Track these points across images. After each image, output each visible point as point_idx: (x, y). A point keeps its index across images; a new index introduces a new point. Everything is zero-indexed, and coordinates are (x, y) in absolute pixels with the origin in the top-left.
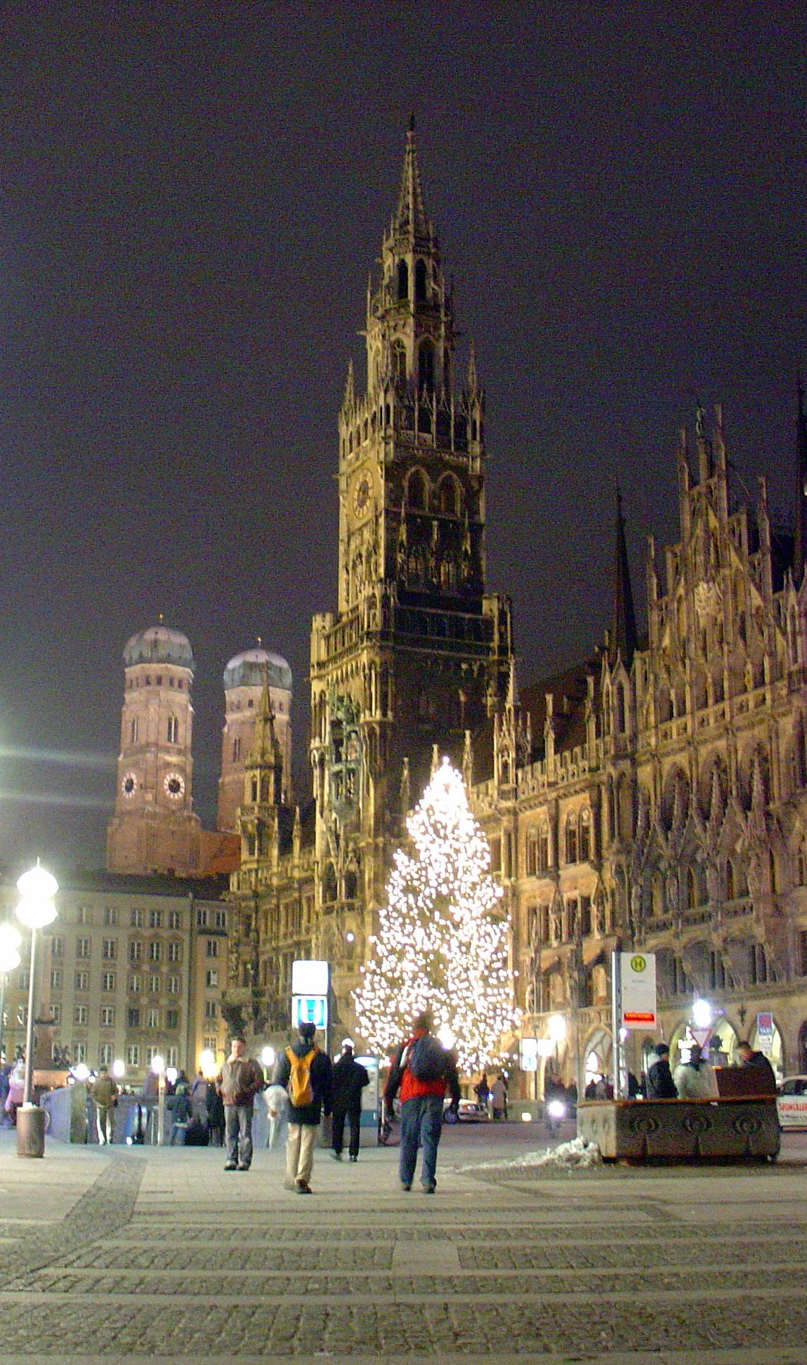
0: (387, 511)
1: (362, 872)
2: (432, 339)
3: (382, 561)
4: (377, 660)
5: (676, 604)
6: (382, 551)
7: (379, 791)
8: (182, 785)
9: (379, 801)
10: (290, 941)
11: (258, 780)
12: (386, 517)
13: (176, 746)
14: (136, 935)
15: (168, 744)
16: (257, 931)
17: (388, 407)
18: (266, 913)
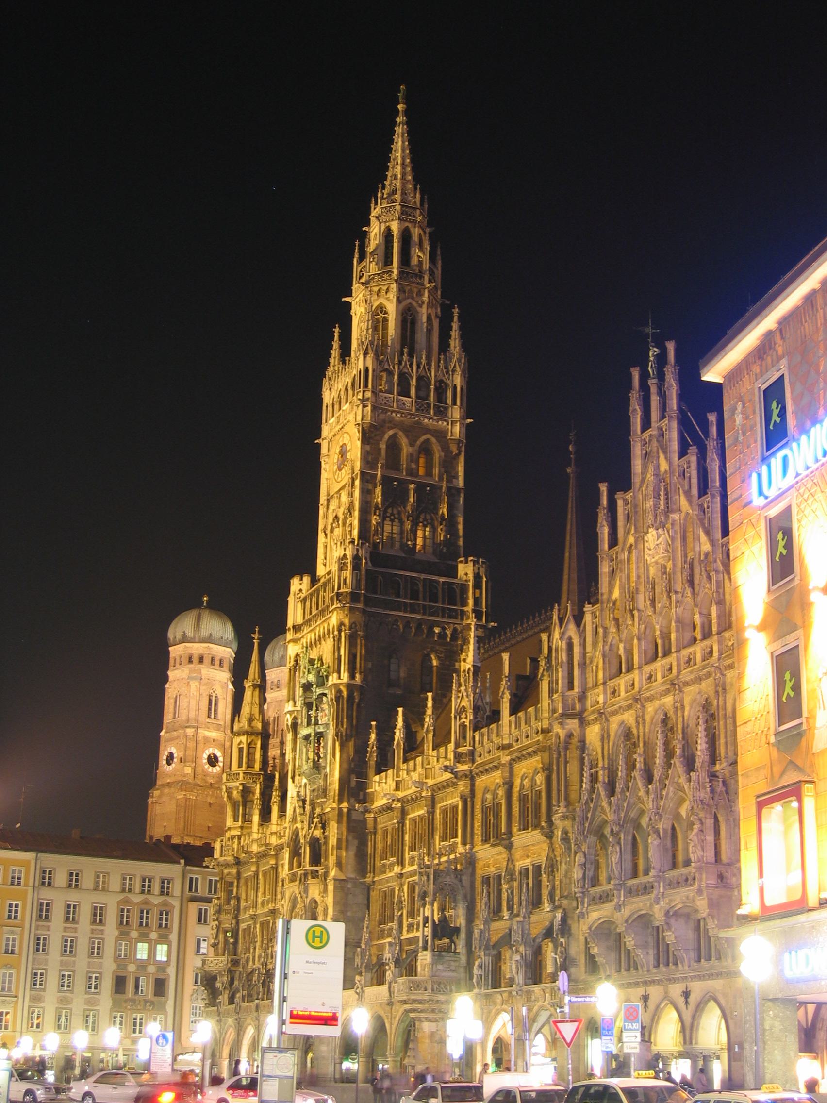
0: (363, 474)
1: (326, 838)
2: (414, 303)
3: (356, 523)
5: (626, 554)
6: (356, 513)
7: (344, 756)
8: (221, 759)
9: (345, 766)
10: (266, 910)
11: (244, 746)
12: (362, 480)
13: (215, 721)
14: (127, 901)
15: (208, 720)
16: (238, 899)
17: (366, 370)
18: (247, 879)
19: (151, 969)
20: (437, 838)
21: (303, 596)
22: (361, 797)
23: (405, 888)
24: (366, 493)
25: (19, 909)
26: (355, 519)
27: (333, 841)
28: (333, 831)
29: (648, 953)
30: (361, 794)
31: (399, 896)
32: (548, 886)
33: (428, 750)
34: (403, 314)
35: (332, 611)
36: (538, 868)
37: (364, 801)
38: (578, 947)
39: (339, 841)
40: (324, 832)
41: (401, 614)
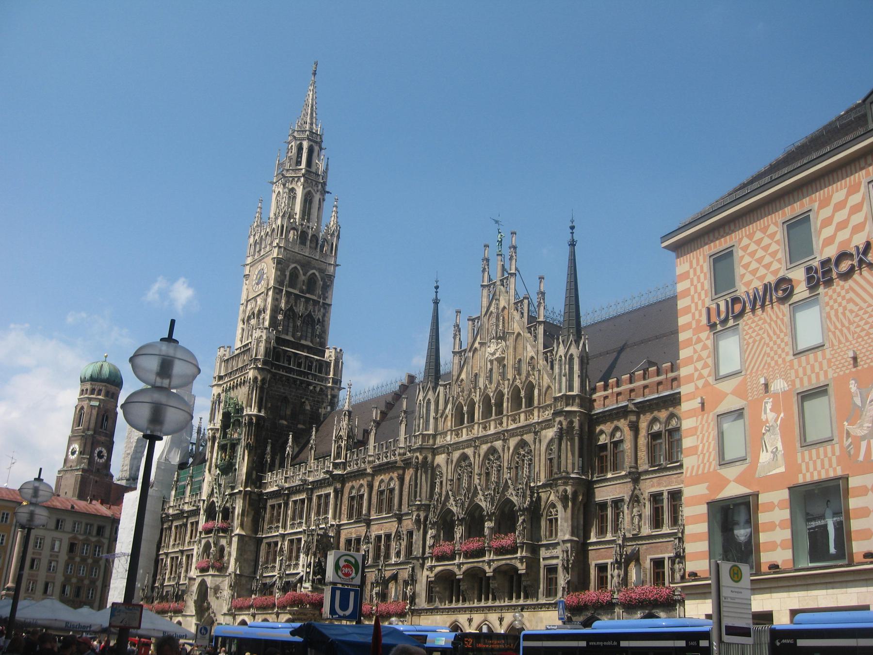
0: (275, 288)
1: (234, 508)
2: (313, 191)
3: (268, 317)
4: (259, 378)
6: (268, 312)
7: (251, 459)
13: (105, 431)
14: (75, 538)
15: (100, 430)
17: (283, 226)
19: (74, 580)
20: (313, 514)
21: (226, 358)
22: (258, 485)
23: (286, 543)
24: (276, 300)
25: (5, 538)
26: (267, 315)
27: (238, 510)
28: (239, 506)
29: (474, 593)
30: (258, 483)
31: (281, 548)
32: (396, 548)
33: (311, 460)
34: (305, 196)
35: (250, 369)
36: (388, 536)
37: (260, 487)
38: (421, 586)
39: (243, 511)
40: (232, 505)
41: (291, 376)
